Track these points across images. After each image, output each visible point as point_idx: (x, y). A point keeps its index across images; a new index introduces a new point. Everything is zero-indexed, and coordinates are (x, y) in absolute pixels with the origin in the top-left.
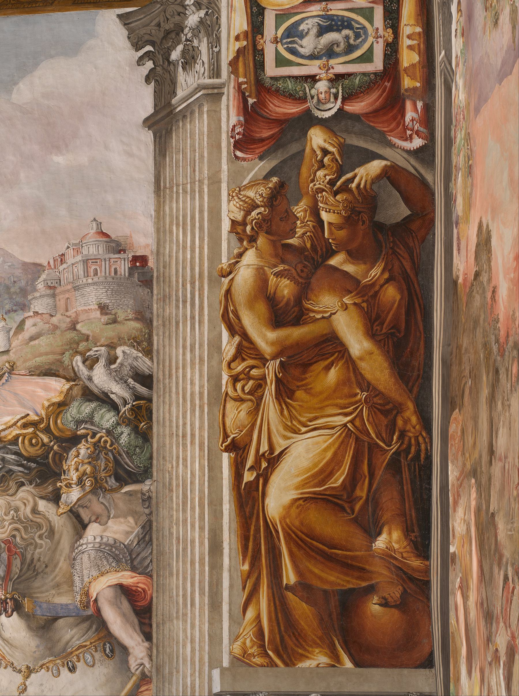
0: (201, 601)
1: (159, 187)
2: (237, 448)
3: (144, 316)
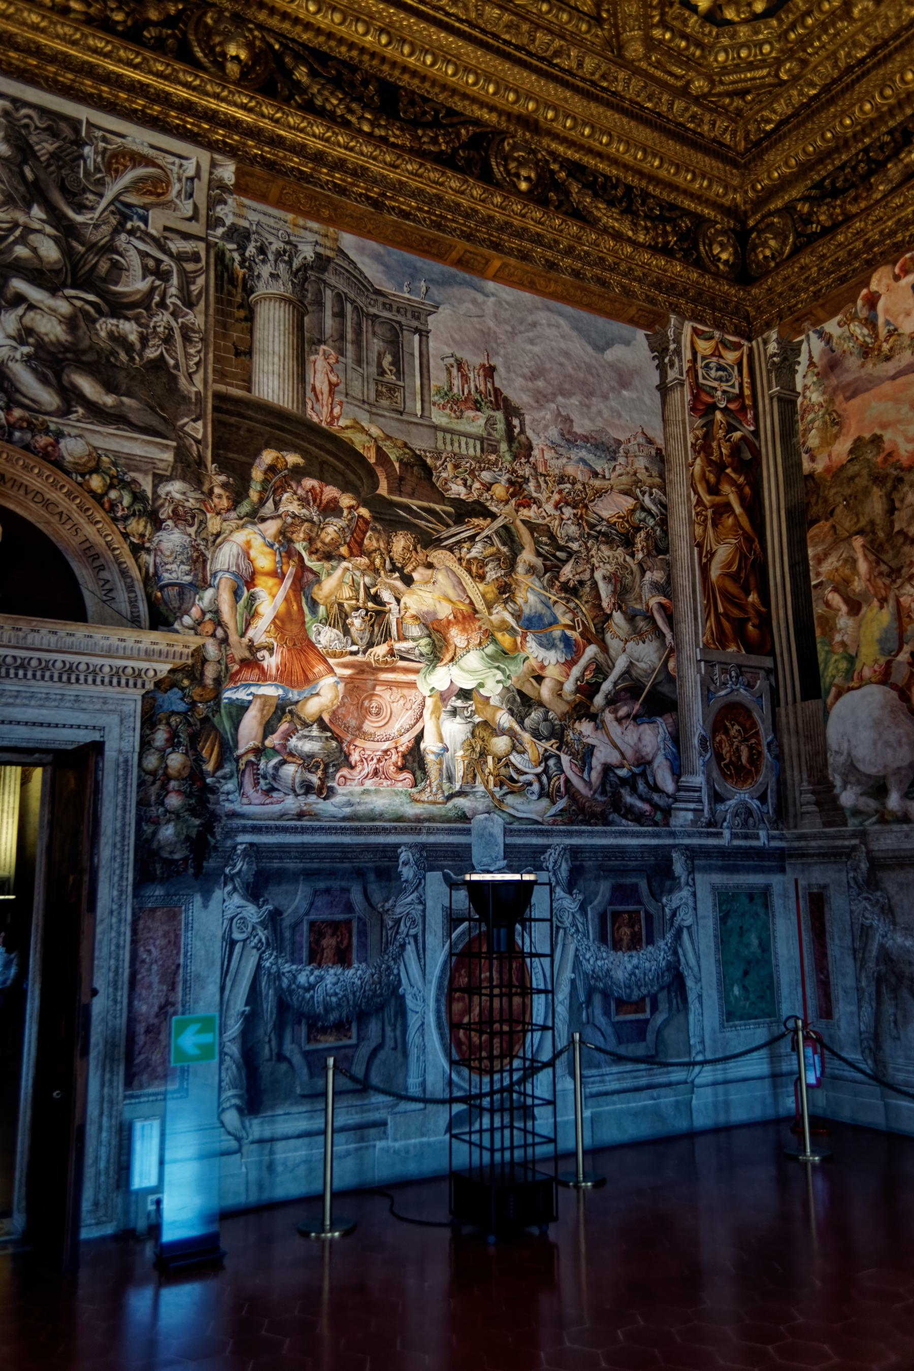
0: (690, 615)
1: (664, 420)
2: (700, 546)
3: (662, 476)
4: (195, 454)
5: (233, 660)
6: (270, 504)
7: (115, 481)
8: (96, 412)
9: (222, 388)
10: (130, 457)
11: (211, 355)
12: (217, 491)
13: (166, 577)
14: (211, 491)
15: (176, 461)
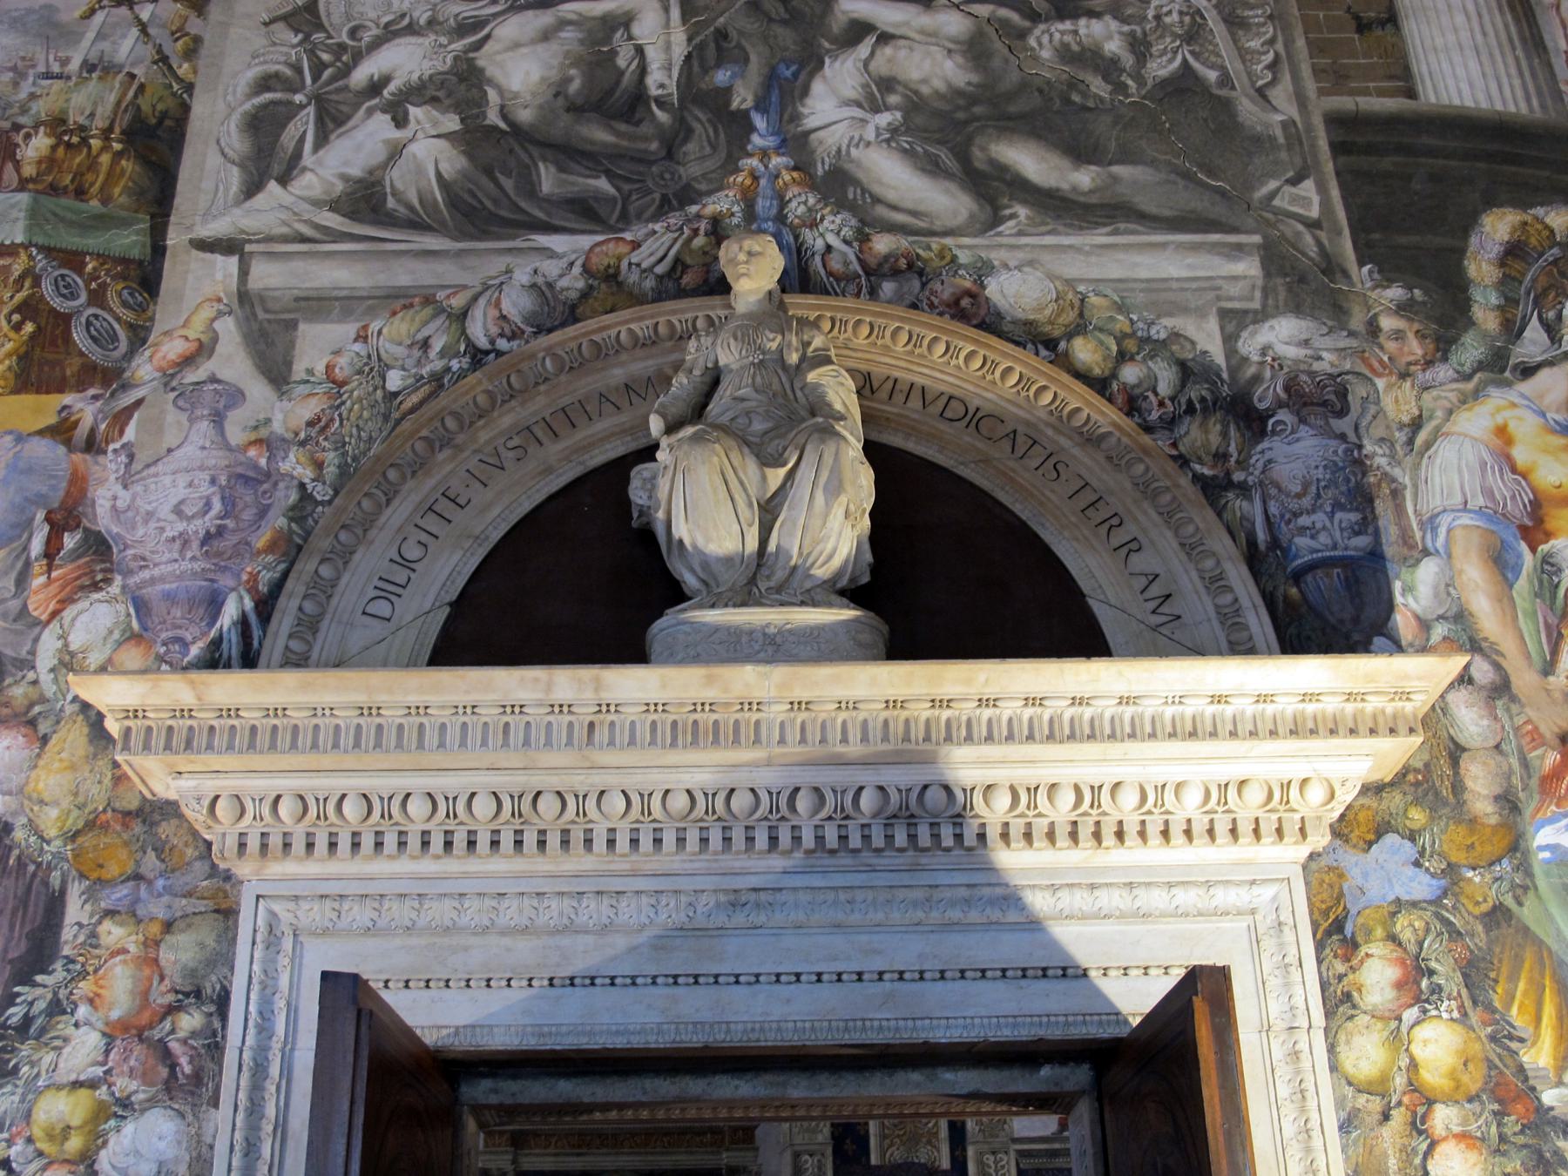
4: (1313, 251)
5: (1537, 738)
6: (1534, 333)
7: (1131, 345)
8: (1059, 208)
9: (1345, 103)
10: (1154, 286)
11: (1301, 43)
12: (1387, 323)
13: (1304, 548)
14: (1373, 329)
15: (1268, 274)
